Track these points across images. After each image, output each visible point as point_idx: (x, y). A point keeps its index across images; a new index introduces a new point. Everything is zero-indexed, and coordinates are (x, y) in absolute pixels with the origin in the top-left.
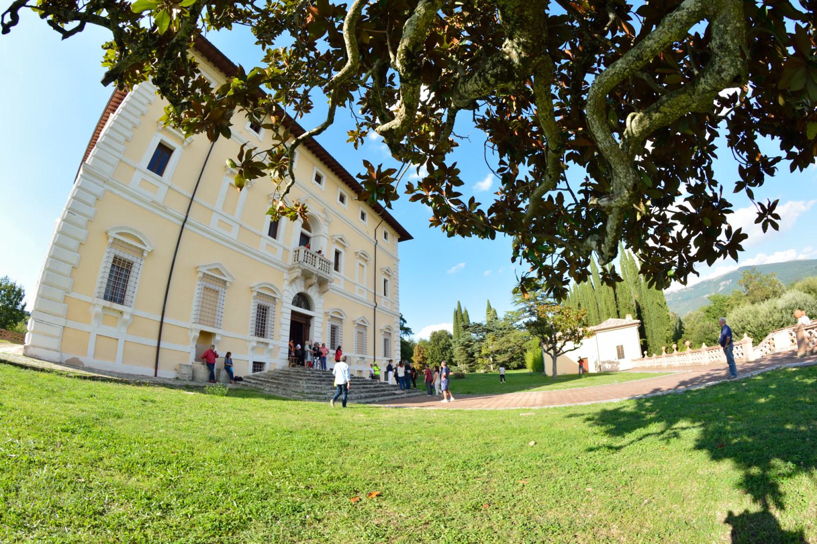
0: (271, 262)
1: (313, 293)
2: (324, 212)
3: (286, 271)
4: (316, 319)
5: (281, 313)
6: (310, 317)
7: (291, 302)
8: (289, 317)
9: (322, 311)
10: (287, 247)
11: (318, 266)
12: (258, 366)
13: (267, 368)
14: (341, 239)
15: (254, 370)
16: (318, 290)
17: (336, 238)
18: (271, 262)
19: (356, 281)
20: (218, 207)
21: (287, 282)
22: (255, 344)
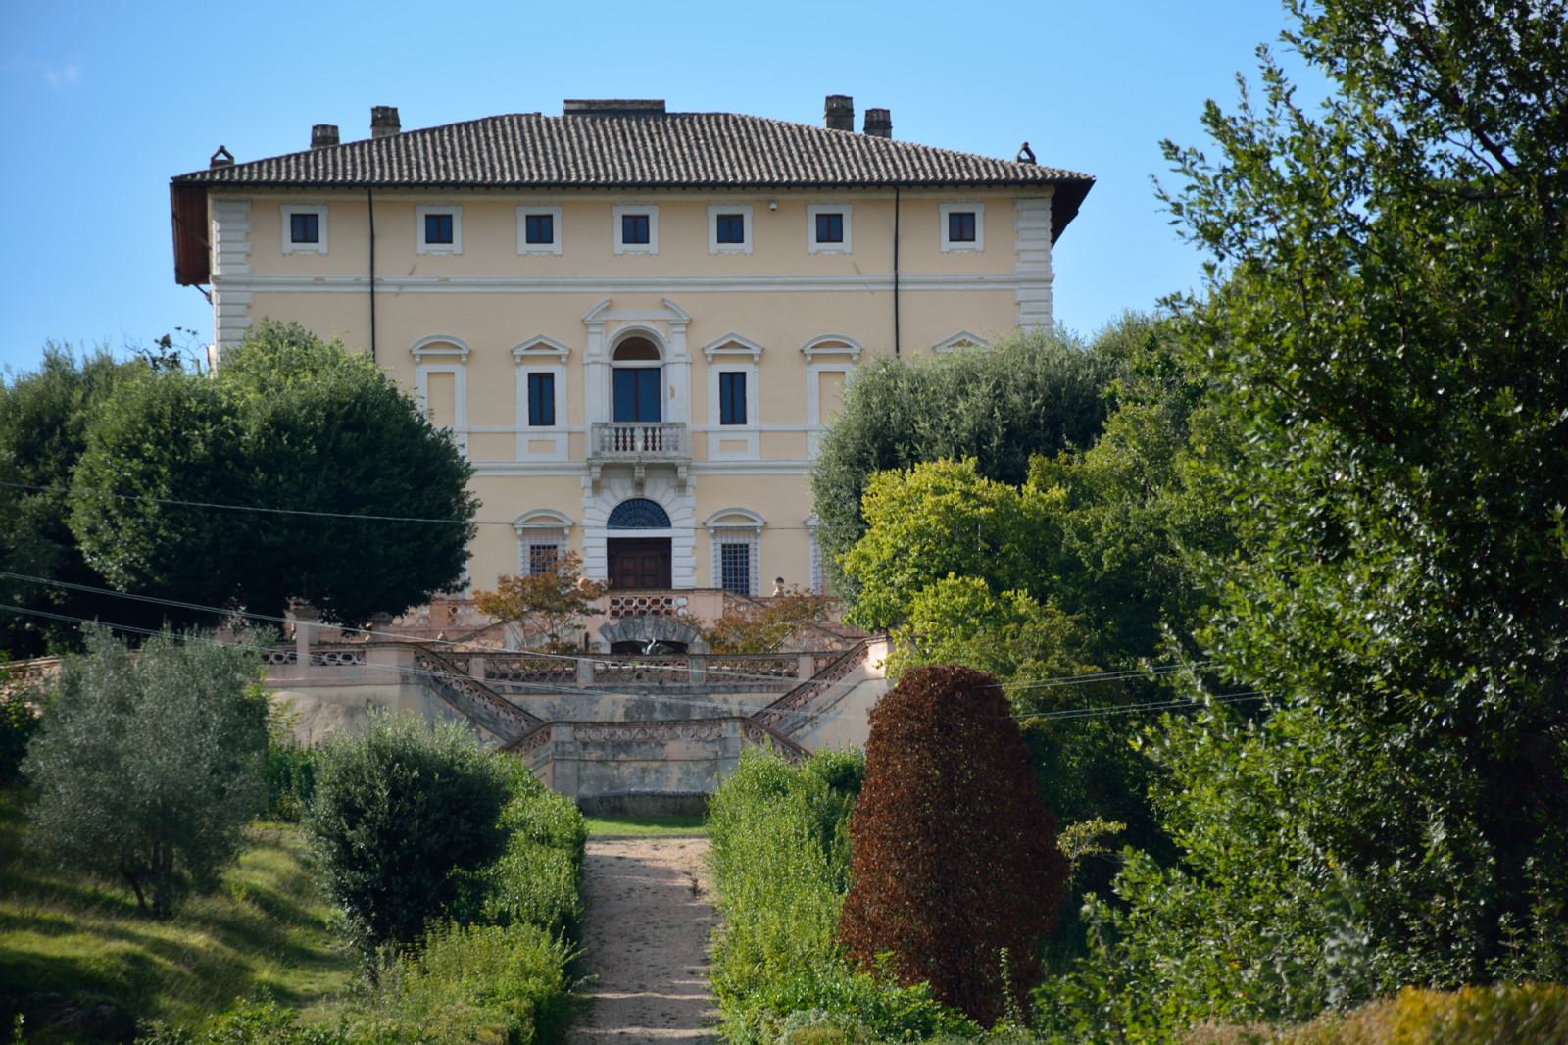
0: (546, 468)
1: (658, 492)
2: (665, 305)
3: (583, 472)
4: (675, 542)
5: (585, 549)
6: (667, 543)
8: (603, 552)
10: (577, 428)
11: (639, 445)
17: (711, 351)
18: (546, 468)
21: (588, 492)
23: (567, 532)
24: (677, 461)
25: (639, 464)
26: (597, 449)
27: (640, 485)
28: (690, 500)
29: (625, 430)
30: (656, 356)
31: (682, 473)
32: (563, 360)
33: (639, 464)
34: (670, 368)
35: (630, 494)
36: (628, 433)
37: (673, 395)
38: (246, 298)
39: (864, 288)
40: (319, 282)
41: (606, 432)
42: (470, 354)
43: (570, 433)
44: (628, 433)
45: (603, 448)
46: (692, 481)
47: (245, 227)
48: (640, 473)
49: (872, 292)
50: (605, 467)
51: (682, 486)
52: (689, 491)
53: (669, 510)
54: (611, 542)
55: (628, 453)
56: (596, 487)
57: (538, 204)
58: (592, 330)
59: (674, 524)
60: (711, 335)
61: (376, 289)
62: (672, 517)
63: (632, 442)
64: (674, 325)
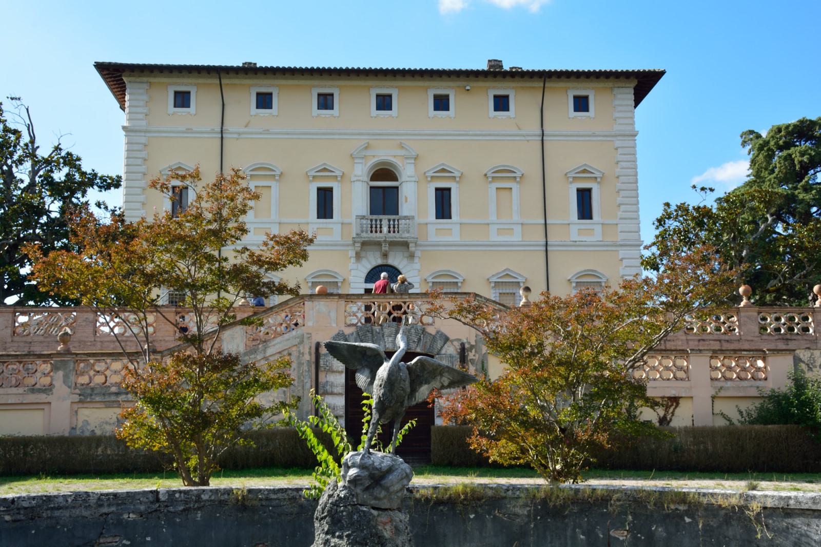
0: (327, 245)
1: (395, 260)
2: (402, 147)
3: (350, 248)
7: (363, 280)
10: (346, 221)
11: (385, 229)
16: (406, 254)
17: (430, 174)
18: (327, 245)
19: (493, 218)
21: (353, 260)
23: (339, 284)
24: (409, 240)
25: (385, 241)
26: (359, 232)
28: (417, 264)
29: (376, 220)
30: (396, 179)
32: (339, 179)
34: (404, 185)
35: (380, 262)
36: (378, 222)
37: (406, 201)
38: (143, 140)
39: (523, 138)
40: (189, 131)
41: (364, 221)
42: (281, 175)
43: (342, 224)
44: (378, 222)
45: (362, 232)
47: (145, 98)
48: (385, 248)
49: (528, 141)
50: (364, 244)
51: (412, 256)
52: (416, 260)
55: (378, 234)
56: (358, 257)
57: (325, 86)
58: (356, 161)
60: (431, 164)
61: (224, 136)
63: (381, 227)
64: (407, 158)
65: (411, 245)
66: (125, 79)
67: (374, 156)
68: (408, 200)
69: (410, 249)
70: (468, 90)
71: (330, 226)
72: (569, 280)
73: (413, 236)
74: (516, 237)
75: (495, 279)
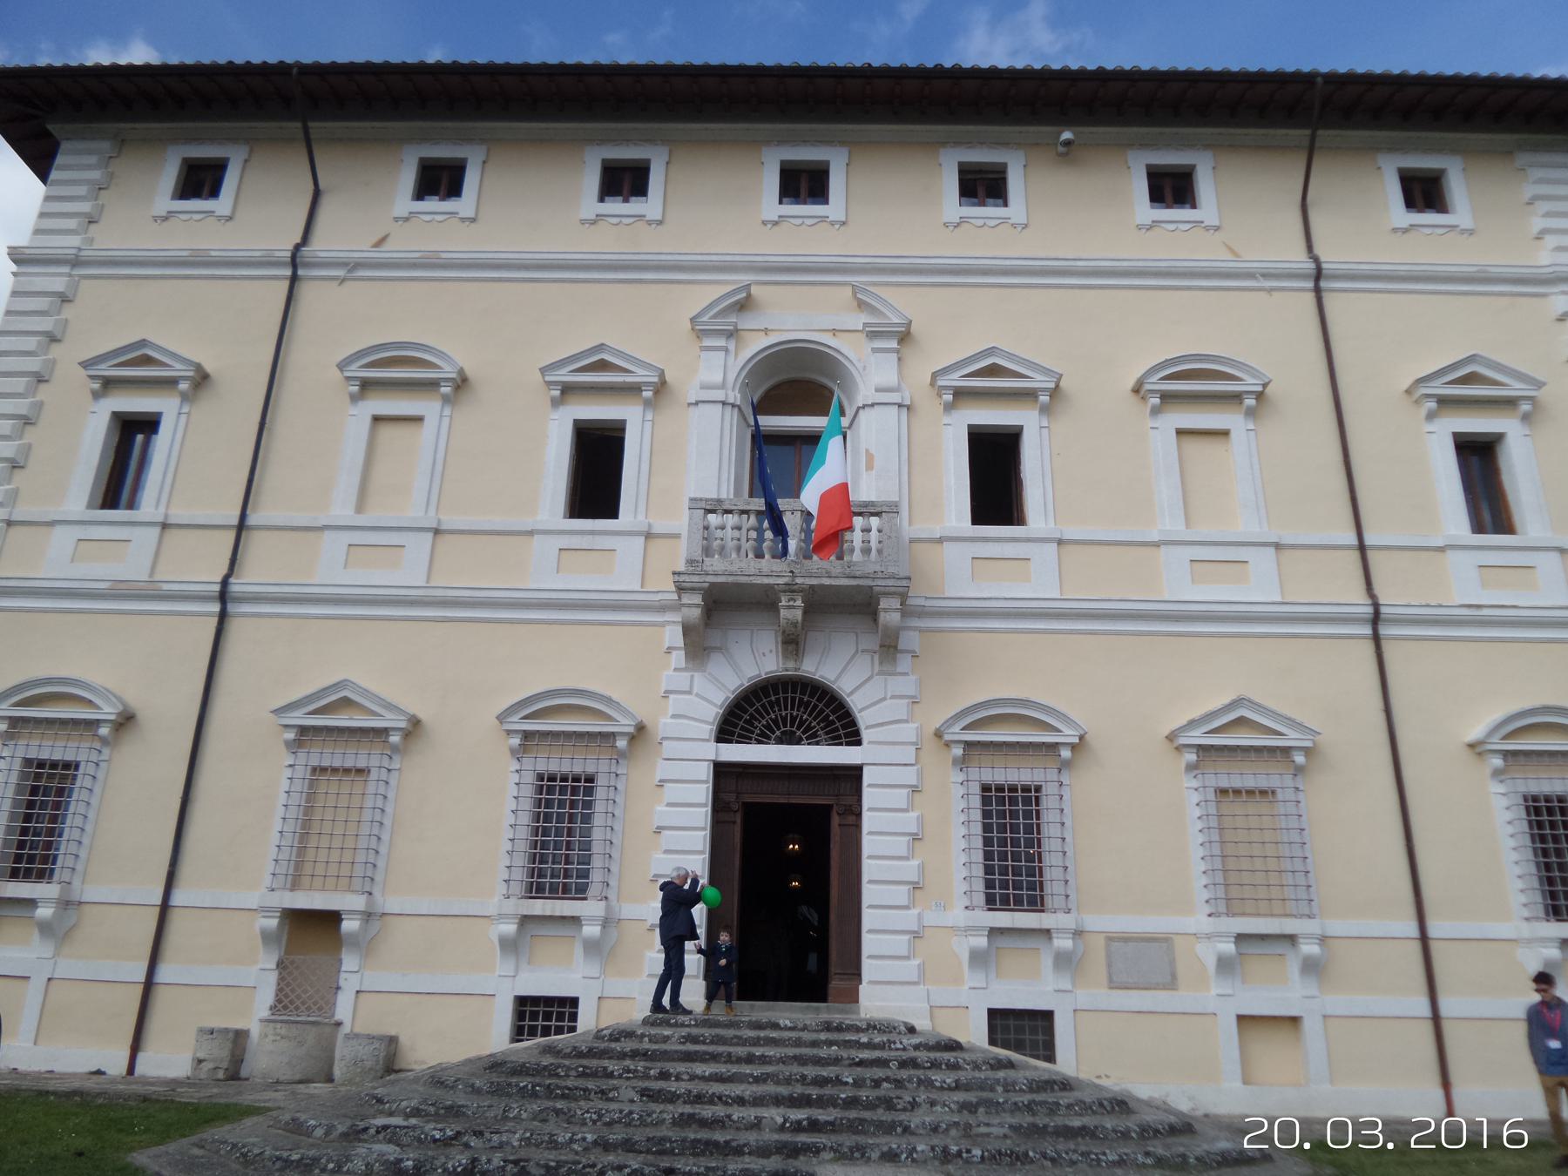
2: (862, 305)
4: (868, 776)
6: (853, 775)
7: (708, 730)
8: (702, 793)
9: (908, 732)
12: (541, 1014)
13: (587, 1020)
14: (993, 371)
15: (518, 1033)
16: (871, 642)
19: (1170, 523)
20: (341, 509)
21: (678, 658)
22: (510, 928)
26: (697, 554)
27: (792, 643)
31: (889, 614)
33: (791, 589)
38: (58, 284)
43: (649, 536)
45: (707, 551)
46: (909, 640)
47: (96, 175)
51: (889, 649)
52: (904, 663)
53: (856, 703)
54: (722, 771)
57: (626, 141)
59: (866, 735)
62: (863, 719)
65: (884, 603)
66: (50, 127)
67: (766, 331)
68: (877, 463)
69: (884, 618)
70: (1068, 143)
71: (607, 542)
72: (1471, 746)
73: (891, 570)
74: (1260, 585)
75: (1197, 737)
